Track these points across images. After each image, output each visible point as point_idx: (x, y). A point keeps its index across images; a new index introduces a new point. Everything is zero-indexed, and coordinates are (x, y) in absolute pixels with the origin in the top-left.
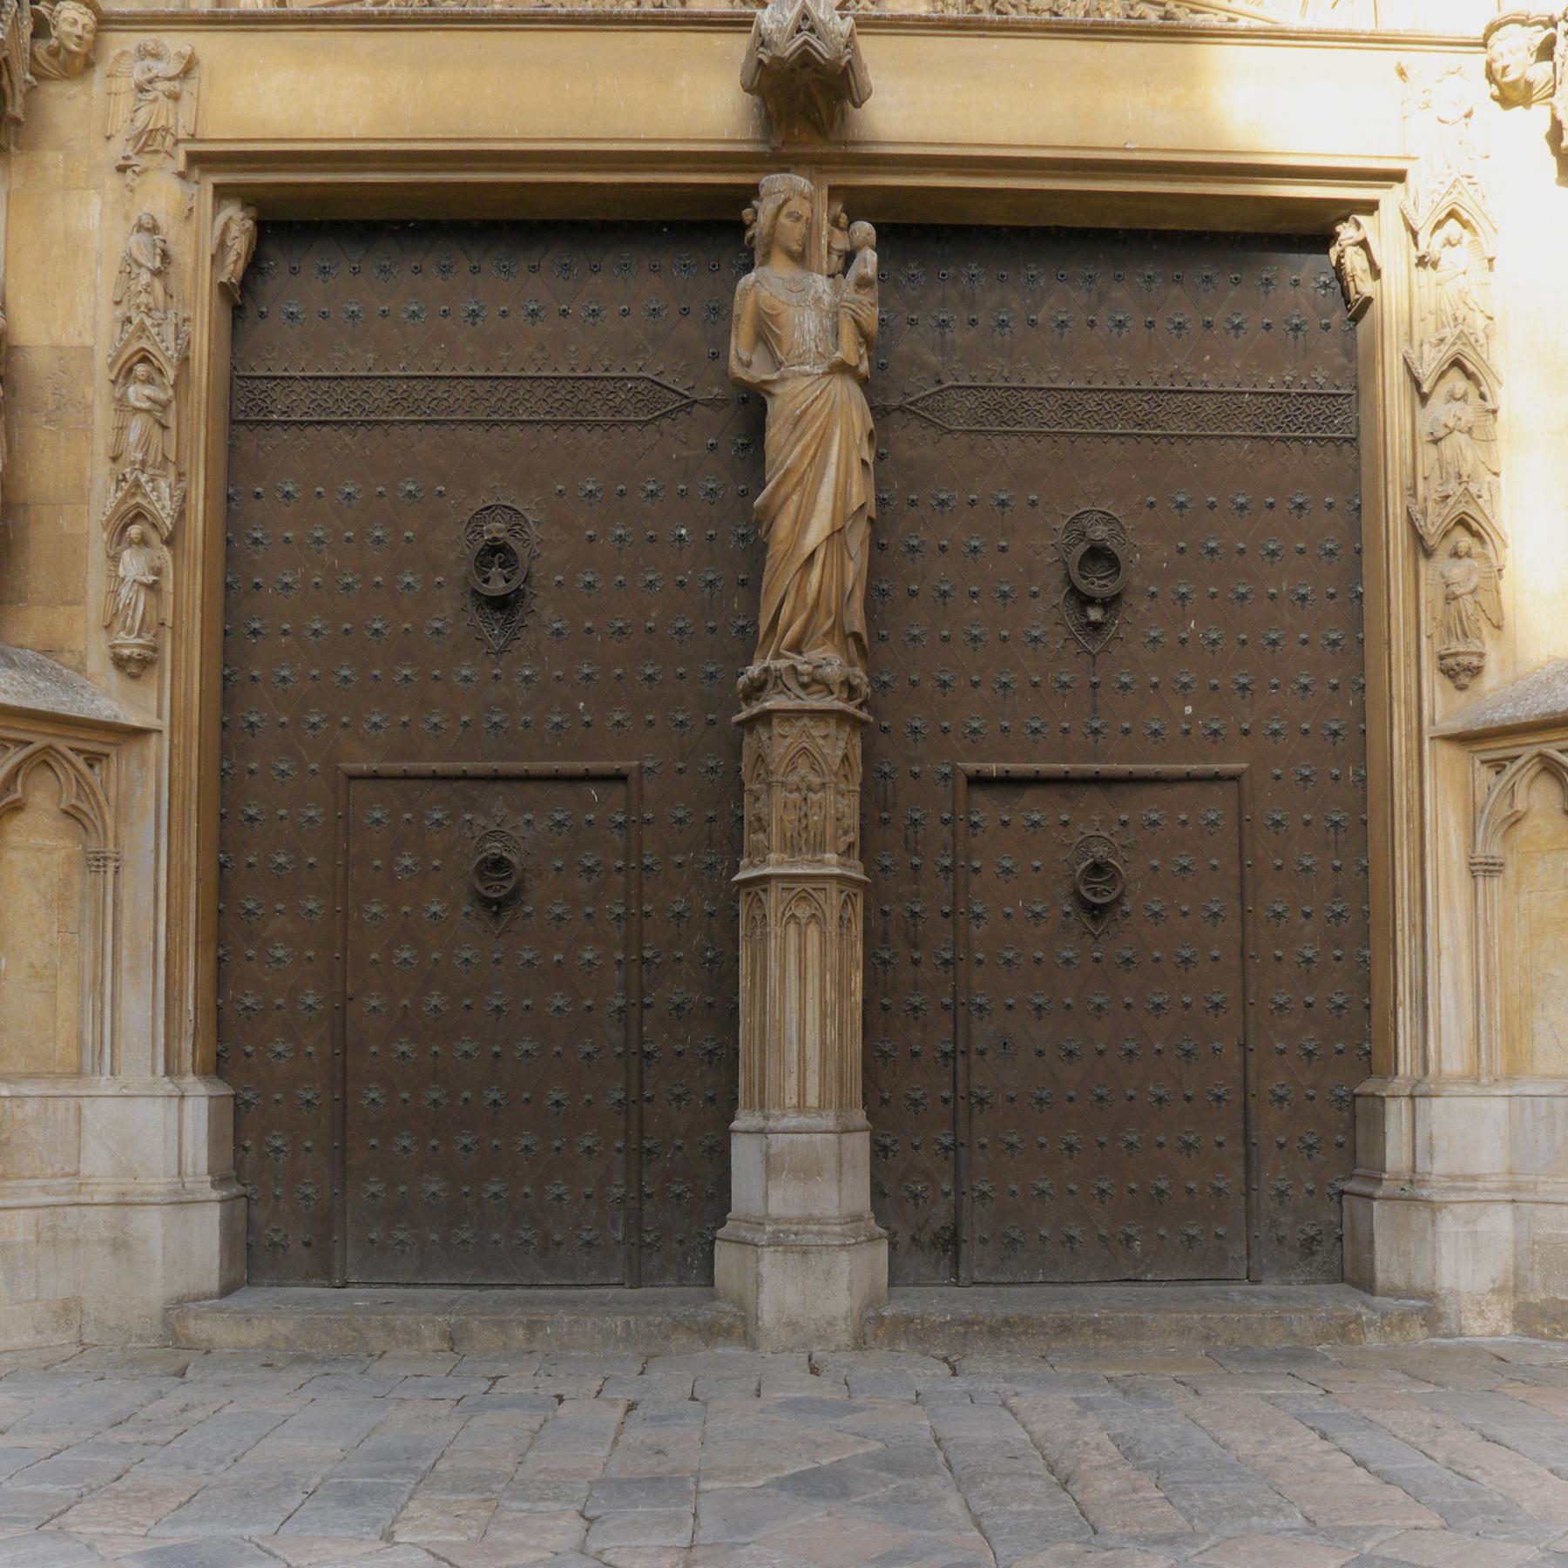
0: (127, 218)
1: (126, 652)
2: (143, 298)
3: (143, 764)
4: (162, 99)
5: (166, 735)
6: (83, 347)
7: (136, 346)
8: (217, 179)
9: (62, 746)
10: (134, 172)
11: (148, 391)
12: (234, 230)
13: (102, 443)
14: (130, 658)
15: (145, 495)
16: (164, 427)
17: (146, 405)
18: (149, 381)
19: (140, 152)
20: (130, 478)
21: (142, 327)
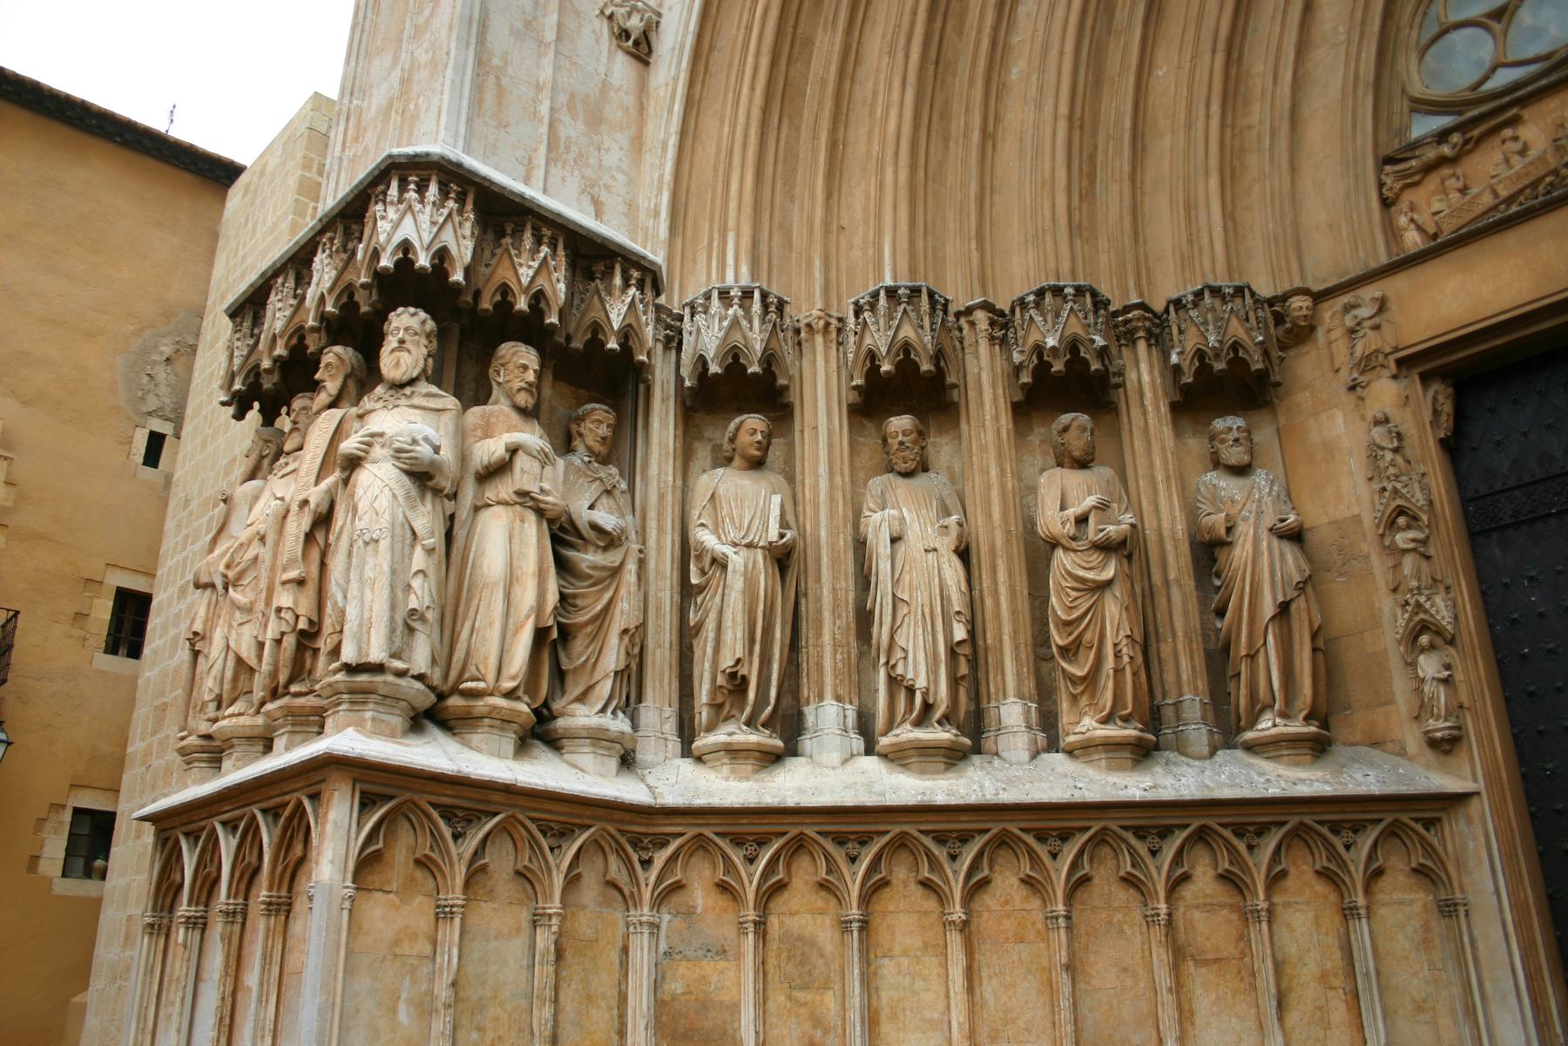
0: (1363, 418)
1: (1439, 735)
2: (1392, 470)
3: (1469, 821)
4: (1370, 333)
5: (1484, 795)
6: (1353, 516)
7: (1394, 505)
8: (1420, 370)
9: (1405, 818)
10: (1363, 387)
11: (1411, 534)
12: (1441, 398)
13: (1382, 580)
14: (1442, 740)
15: (1426, 611)
16: (1428, 558)
17: (1412, 545)
18: (1408, 527)
19: (1362, 373)
20: (1412, 601)
21: (1395, 491)
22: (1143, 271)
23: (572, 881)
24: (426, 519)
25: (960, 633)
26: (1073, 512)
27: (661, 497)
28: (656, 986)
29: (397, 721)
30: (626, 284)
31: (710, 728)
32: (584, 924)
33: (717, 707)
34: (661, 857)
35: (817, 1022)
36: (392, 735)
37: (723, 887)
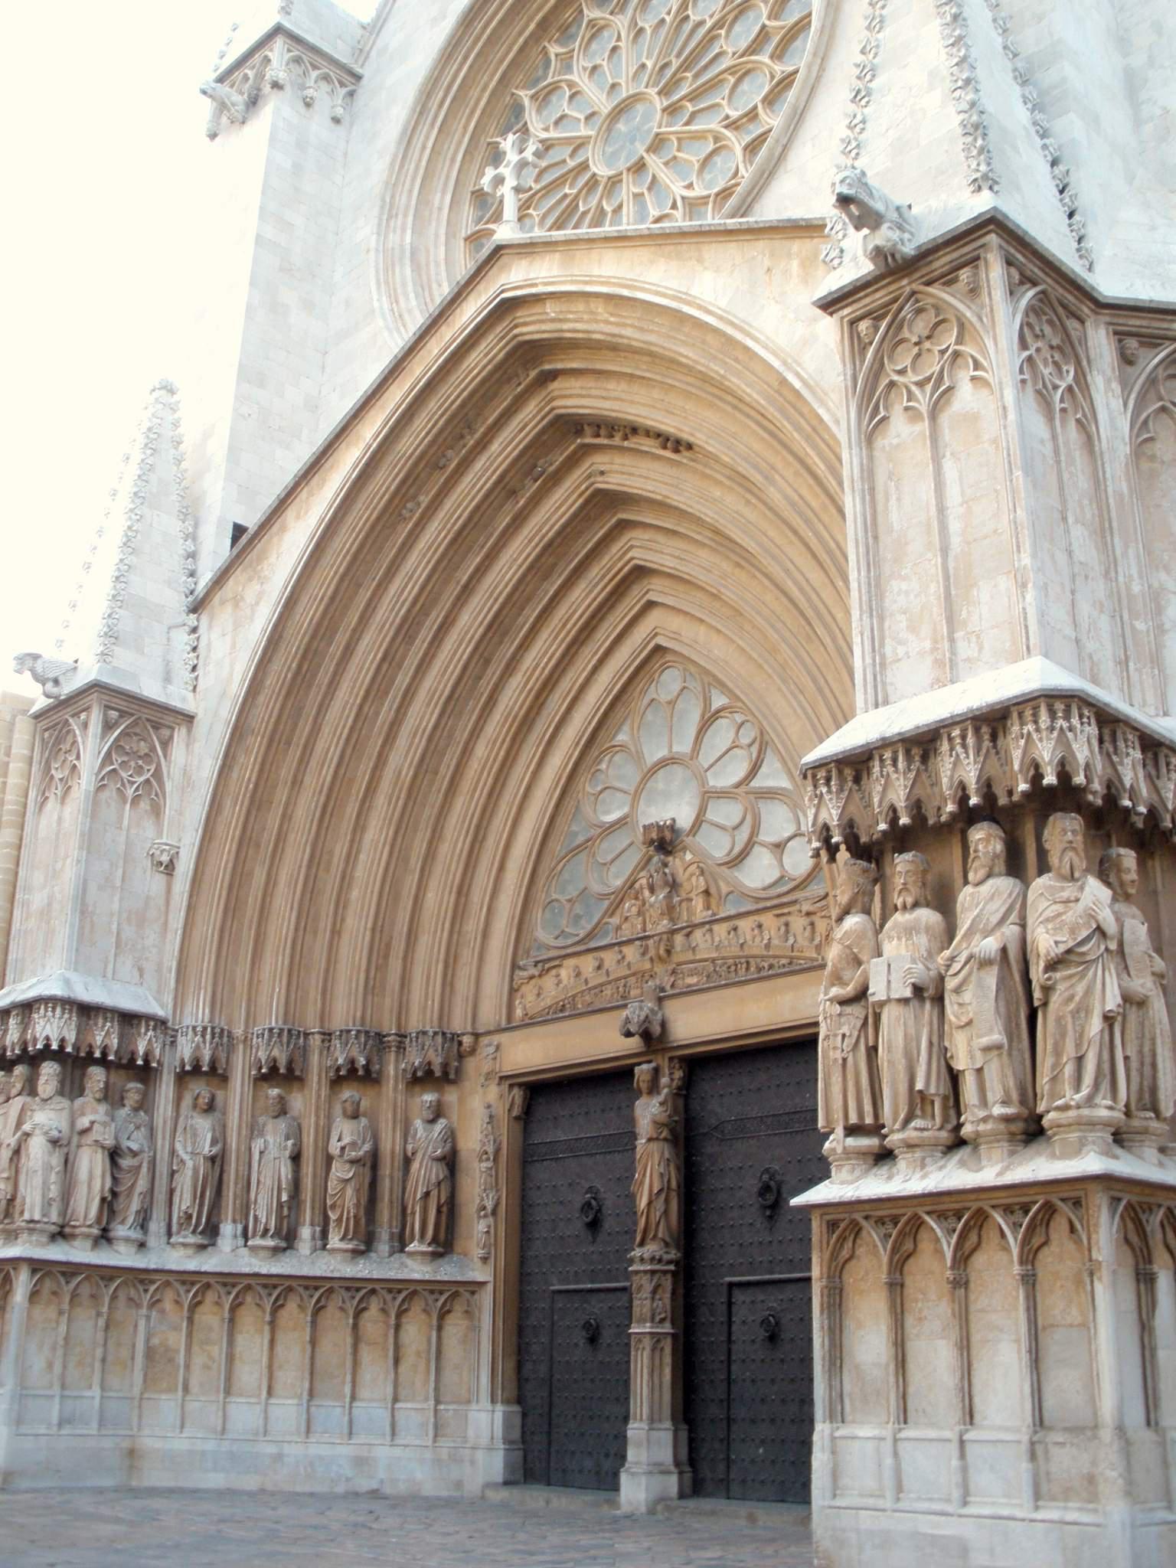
22: (402, 1009)
23: (114, 1297)
24: (56, 1161)
25: (284, 1198)
26: (342, 1143)
27: (165, 1122)
28: (148, 1340)
29: (44, 1239)
30: (147, 1030)
31: (179, 1233)
32: (119, 1315)
33: (180, 1225)
34: (152, 1288)
35: (210, 1358)
36: (43, 1245)
37: (177, 1302)
